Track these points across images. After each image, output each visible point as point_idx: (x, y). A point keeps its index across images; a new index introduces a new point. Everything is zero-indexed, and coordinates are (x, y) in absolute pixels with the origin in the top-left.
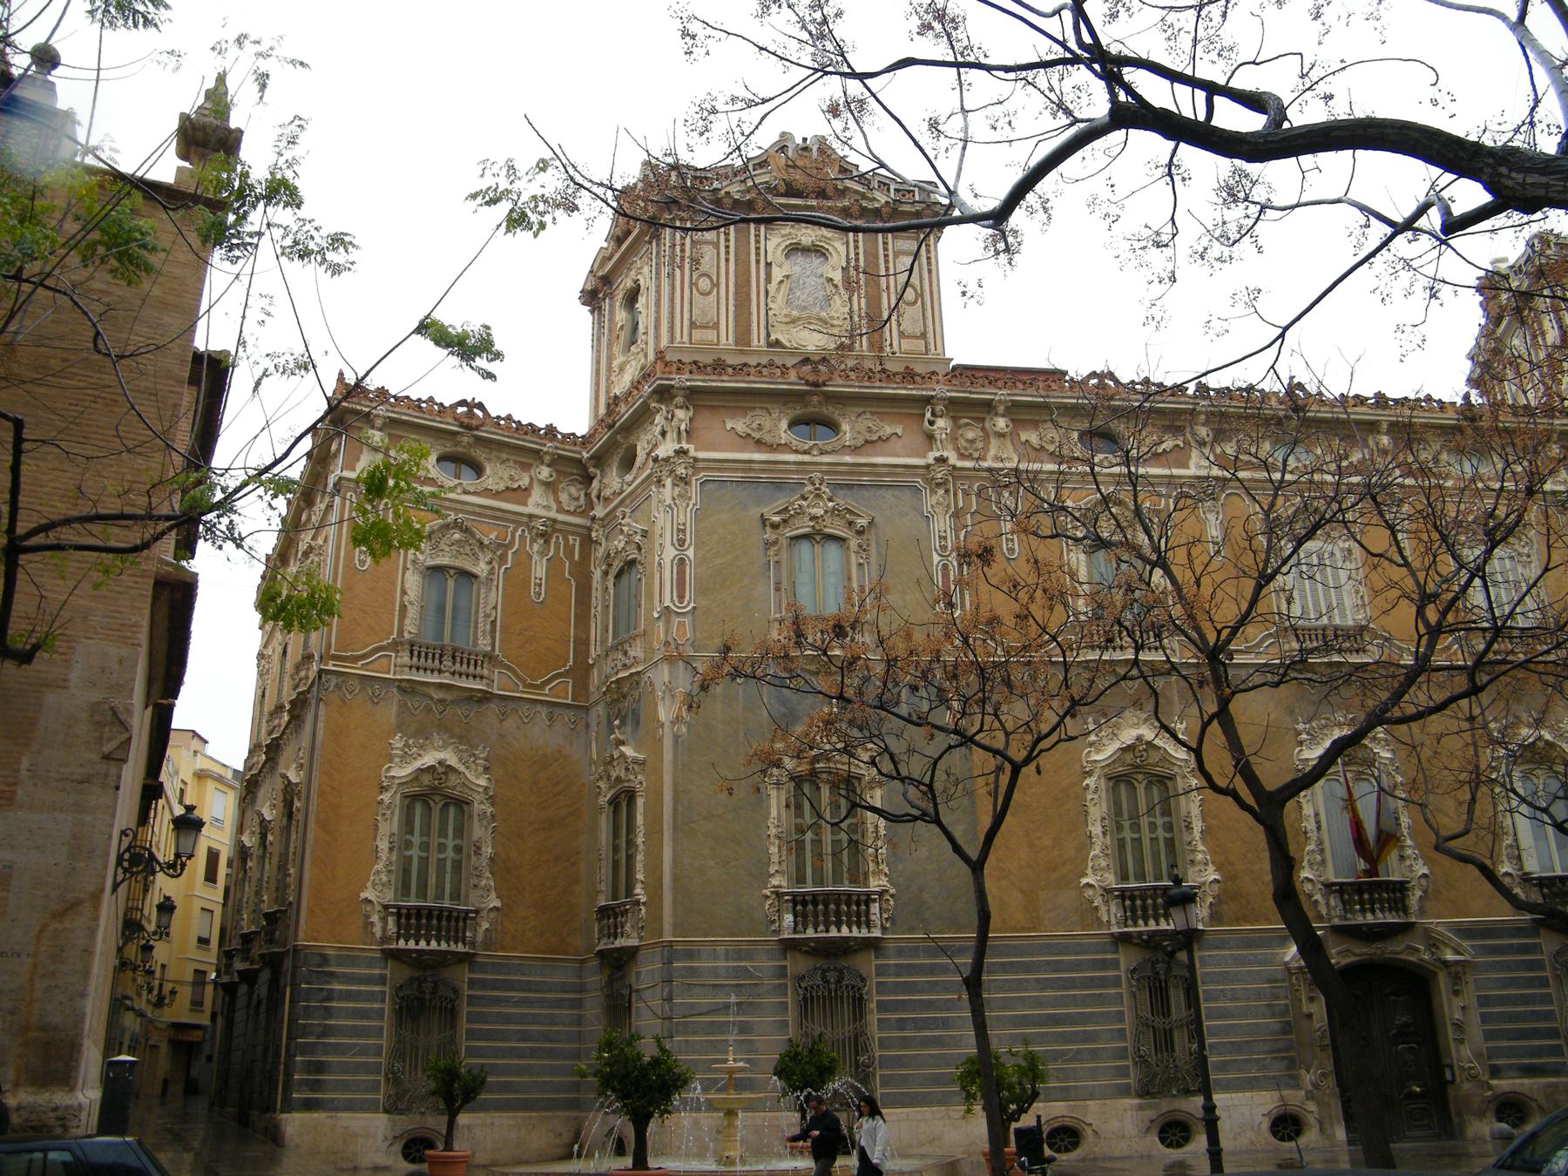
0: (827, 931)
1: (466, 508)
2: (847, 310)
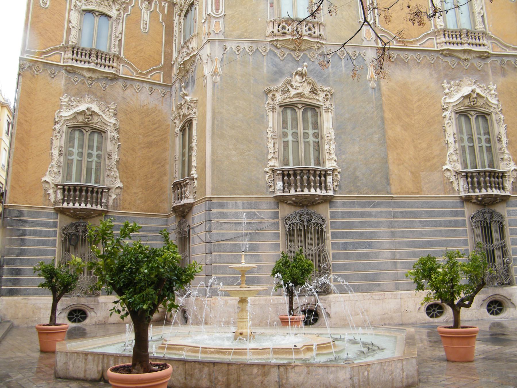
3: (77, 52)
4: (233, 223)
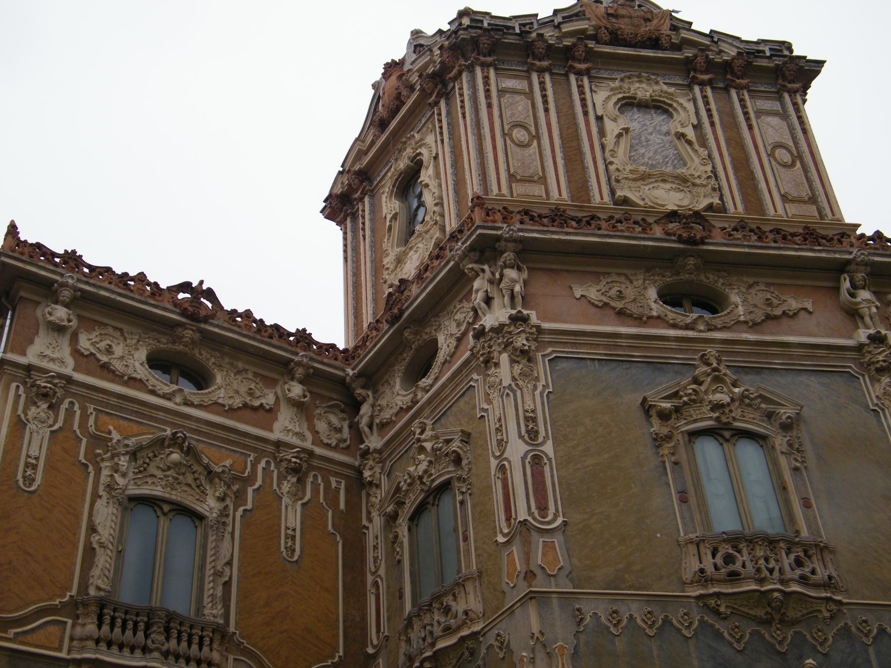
1: (187, 423)
2: (709, 168)
3: (113, 619)
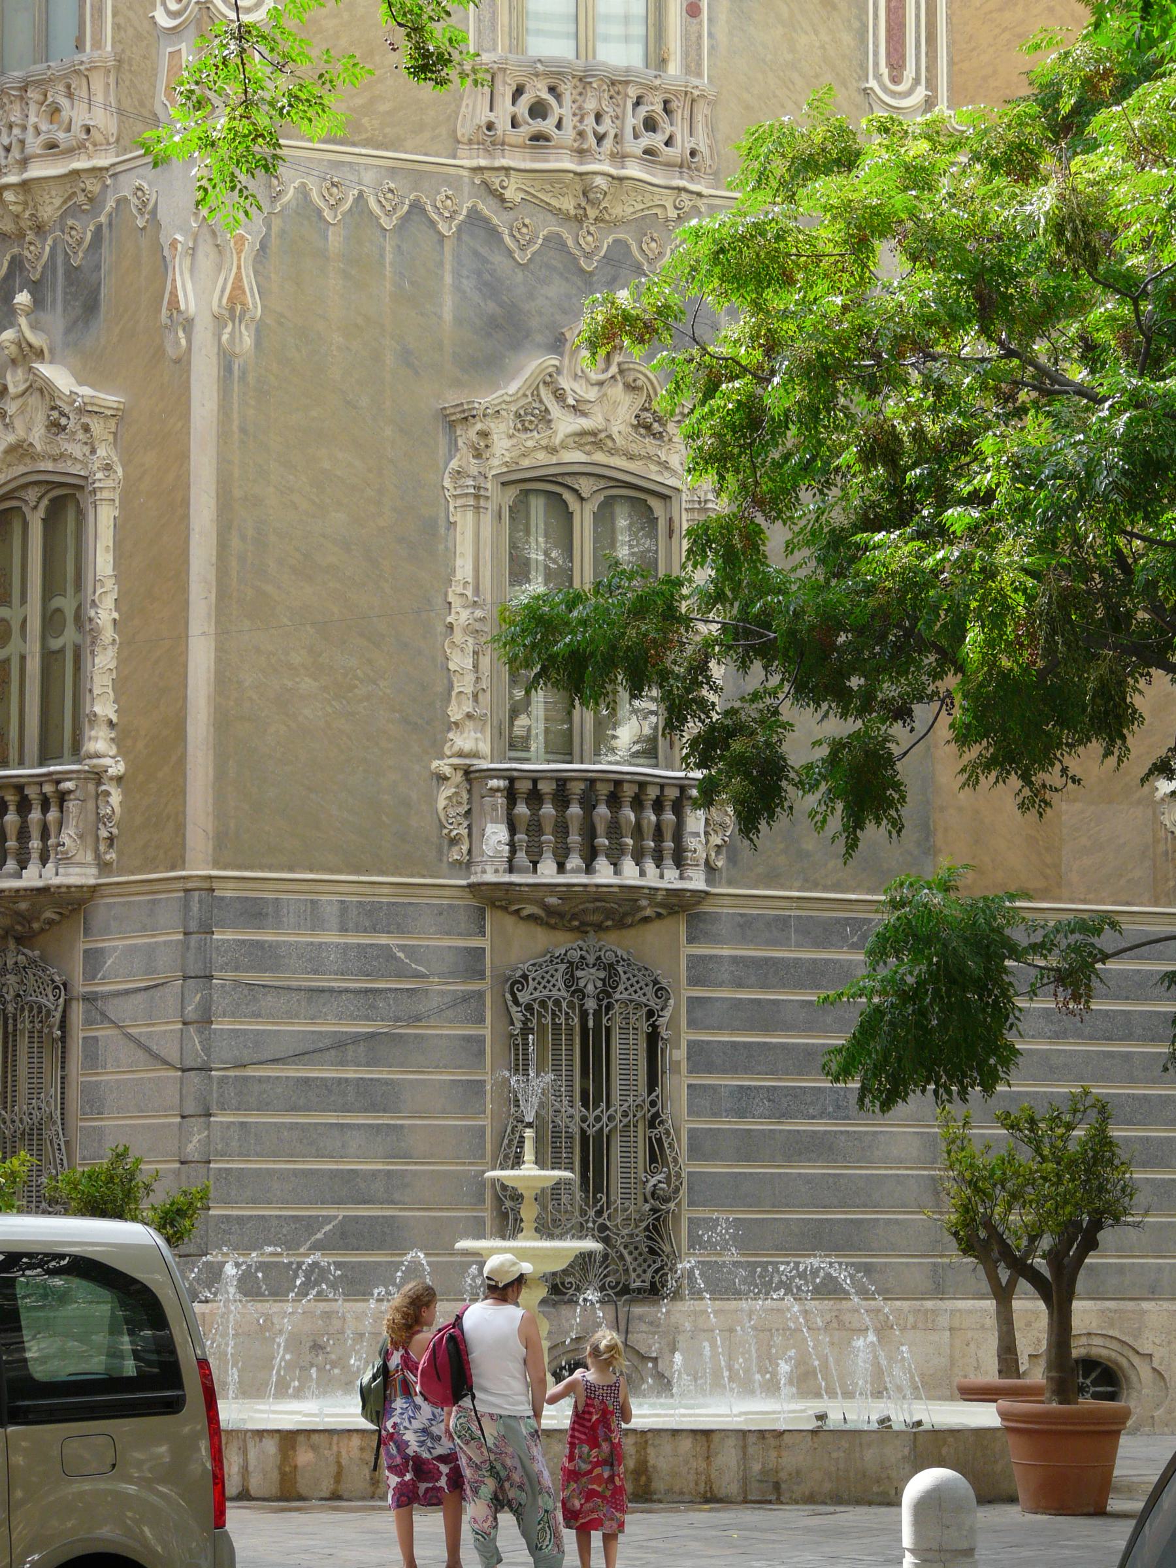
0: (589, 869)
4: (299, 989)
